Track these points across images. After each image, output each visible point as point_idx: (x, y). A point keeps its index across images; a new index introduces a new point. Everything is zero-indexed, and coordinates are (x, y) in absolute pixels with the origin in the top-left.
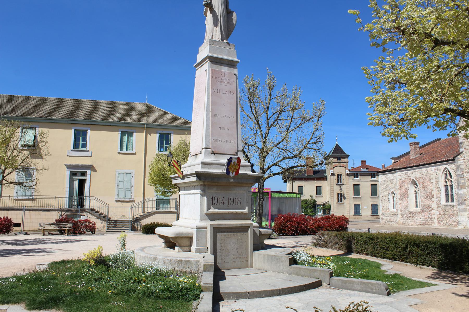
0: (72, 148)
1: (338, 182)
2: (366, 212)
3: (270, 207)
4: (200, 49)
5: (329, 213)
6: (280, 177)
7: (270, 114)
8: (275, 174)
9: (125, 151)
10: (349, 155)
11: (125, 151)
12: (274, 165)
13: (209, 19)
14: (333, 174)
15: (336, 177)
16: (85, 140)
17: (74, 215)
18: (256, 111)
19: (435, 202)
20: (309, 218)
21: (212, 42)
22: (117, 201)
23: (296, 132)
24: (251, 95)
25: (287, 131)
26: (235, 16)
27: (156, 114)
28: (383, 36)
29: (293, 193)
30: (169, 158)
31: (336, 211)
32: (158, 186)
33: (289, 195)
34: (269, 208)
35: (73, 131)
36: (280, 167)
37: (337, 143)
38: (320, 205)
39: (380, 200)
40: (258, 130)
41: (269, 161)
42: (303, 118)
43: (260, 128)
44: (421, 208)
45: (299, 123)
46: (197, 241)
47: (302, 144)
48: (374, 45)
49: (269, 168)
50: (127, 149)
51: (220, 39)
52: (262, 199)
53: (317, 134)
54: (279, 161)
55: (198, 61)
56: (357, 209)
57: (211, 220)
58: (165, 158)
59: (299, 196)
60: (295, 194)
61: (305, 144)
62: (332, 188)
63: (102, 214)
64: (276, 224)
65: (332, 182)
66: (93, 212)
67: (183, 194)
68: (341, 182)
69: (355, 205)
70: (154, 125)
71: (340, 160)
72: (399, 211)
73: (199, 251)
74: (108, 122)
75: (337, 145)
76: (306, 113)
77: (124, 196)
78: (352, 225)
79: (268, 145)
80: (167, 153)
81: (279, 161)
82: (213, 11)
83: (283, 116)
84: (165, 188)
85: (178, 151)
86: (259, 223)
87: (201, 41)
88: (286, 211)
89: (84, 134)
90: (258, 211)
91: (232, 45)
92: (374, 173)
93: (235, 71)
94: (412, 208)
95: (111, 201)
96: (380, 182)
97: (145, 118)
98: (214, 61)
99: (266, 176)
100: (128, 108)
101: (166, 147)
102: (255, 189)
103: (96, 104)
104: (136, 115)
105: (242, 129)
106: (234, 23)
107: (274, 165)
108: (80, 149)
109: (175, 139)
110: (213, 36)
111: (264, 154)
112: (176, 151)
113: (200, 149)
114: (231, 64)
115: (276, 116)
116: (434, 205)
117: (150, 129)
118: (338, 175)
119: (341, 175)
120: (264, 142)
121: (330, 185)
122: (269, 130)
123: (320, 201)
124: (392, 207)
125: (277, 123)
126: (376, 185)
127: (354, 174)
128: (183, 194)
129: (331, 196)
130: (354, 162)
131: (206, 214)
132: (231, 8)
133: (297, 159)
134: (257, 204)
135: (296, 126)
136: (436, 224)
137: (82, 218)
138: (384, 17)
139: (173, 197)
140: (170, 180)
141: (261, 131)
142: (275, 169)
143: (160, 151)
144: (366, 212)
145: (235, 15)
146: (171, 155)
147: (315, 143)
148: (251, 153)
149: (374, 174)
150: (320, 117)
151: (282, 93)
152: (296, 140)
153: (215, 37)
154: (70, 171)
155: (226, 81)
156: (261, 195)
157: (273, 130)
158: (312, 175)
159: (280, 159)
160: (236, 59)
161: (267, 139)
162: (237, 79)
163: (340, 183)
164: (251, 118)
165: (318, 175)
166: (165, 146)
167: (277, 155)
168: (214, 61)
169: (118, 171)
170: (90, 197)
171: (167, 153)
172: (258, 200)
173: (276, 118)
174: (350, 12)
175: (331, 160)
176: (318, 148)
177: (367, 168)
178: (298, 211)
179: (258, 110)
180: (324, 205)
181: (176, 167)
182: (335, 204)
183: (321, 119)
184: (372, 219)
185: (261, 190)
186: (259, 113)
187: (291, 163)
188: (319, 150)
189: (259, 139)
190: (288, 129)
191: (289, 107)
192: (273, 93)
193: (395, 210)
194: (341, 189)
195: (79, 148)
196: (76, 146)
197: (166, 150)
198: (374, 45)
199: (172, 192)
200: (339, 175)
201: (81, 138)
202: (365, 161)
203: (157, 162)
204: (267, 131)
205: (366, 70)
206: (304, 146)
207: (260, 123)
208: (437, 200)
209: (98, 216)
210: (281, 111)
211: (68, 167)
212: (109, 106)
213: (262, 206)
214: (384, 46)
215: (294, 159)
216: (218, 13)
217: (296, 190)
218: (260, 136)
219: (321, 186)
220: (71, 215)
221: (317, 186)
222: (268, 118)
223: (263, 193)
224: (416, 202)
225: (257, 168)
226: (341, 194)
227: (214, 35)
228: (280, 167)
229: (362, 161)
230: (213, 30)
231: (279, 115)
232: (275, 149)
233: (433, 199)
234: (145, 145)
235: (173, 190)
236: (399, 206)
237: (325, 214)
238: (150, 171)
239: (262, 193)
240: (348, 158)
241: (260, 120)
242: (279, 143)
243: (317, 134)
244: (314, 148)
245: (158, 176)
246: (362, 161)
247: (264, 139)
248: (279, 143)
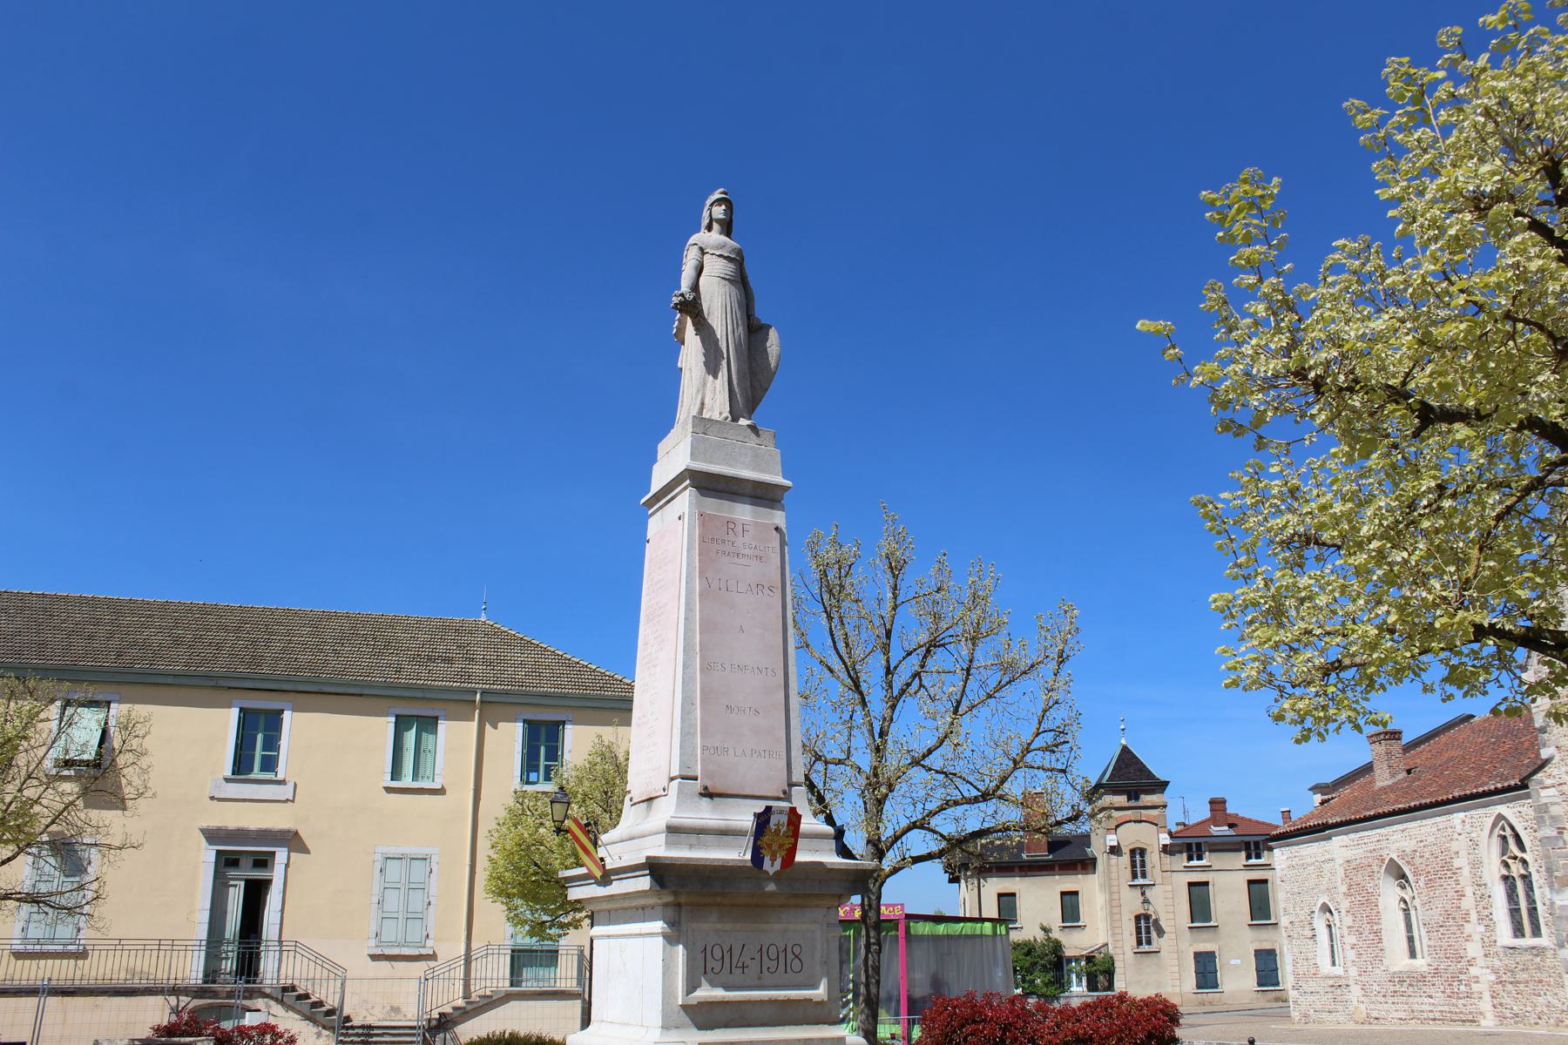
0: (229, 773)
1: (1134, 876)
2: (1238, 978)
3: (903, 973)
4: (662, 447)
5: (1110, 987)
6: (936, 867)
7: (896, 654)
8: (917, 860)
9: (407, 781)
10: (1166, 783)
11: (407, 781)
12: (913, 826)
13: (692, 352)
14: (1115, 850)
15: (1126, 859)
16: (272, 743)
17: (221, 1006)
18: (847, 645)
19: (1477, 937)
20: (1039, 1008)
21: (702, 423)
22: (374, 957)
23: (984, 711)
24: (833, 592)
25: (955, 712)
26: (773, 341)
27: (516, 655)
28: (1255, 400)
29: (982, 920)
30: (556, 806)
31: (1133, 981)
32: (520, 902)
33: (967, 928)
34: (903, 973)
35: (234, 713)
36: (935, 832)
37: (1123, 742)
38: (1077, 959)
39: (1284, 935)
40: (859, 708)
41: (896, 814)
42: (1007, 667)
43: (864, 703)
44: (1429, 960)
45: (992, 684)
47: (1006, 754)
48: (1226, 428)
49: (897, 838)
50: (415, 776)
51: (726, 413)
52: (875, 948)
53: (1057, 717)
54: (932, 814)
55: (656, 486)
56: (1206, 970)
57: (703, 1026)
58: (543, 806)
59: (1002, 930)
60: (988, 925)
61: (1015, 752)
62: (1115, 896)
63: (320, 1004)
64: (927, 1031)
65: (1114, 875)
66: (289, 995)
67: (602, 937)
68: (1144, 875)
69: (1197, 955)
70: (507, 693)
71: (1137, 798)
74: (354, 684)
75: (1125, 750)
76: (1016, 647)
77: (400, 938)
78: (1192, 1026)
79: (893, 760)
80: (550, 787)
81: (932, 814)
82: (702, 327)
83: (938, 660)
84: (543, 909)
85: (587, 784)
86: (865, 1037)
87: (665, 423)
88: (959, 986)
89: (273, 722)
90: (862, 989)
91: (766, 435)
92: (1255, 842)
93: (779, 518)
94: (1398, 960)
95: (355, 959)
96: (1278, 873)
97: (477, 669)
98: (709, 485)
99: (887, 864)
100: (422, 637)
101: (548, 769)
102: (853, 910)
103: (317, 622)
104: (449, 660)
105: (804, 706)
106: (773, 361)
107: (913, 826)
108: (256, 774)
109: (579, 742)
110: (703, 404)
111: (878, 791)
112: (580, 781)
113: (662, 777)
114: (764, 495)
115: (914, 661)
116: (1474, 949)
117: (493, 706)
118: (1133, 852)
119: (1142, 852)
120: (878, 749)
121: (1108, 887)
122: (893, 707)
123: (1075, 944)
125: (921, 686)
126: (1265, 881)
127: (1189, 847)
128: (602, 937)
129: (1114, 927)
130: (1185, 806)
131: (684, 1007)
132: (761, 314)
133: (991, 806)
134: (860, 961)
135: (982, 694)
136: (1489, 1015)
137: (250, 1020)
138: (1254, 342)
139: (569, 942)
140: (563, 884)
141: (868, 714)
142: (918, 842)
143: (528, 783)
144: (1238, 978)
145: (773, 337)
146: (563, 797)
147: (1049, 749)
148: (834, 785)
149: (1257, 844)
150: (1062, 659)
151: (934, 583)
152: (985, 739)
153: (712, 409)
154: (218, 852)
156: (872, 933)
157: (907, 706)
158: (1044, 855)
159: (932, 806)
160: (779, 479)
161: (890, 738)
162: (783, 544)
163: (1140, 881)
164: (831, 671)
165: (1064, 854)
166: (542, 763)
167: (922, 793)
168: (709, 485)
170: (280, 941)
171: (550, 787)
172: (863, 951)
173: (917, 668)
174: (1145, 329)
175: (1108, 799)
176: (1060, 767)
177: (1231, 826)
178: (1001, 984)
179: (859, 644)
180: (1090, 959)
181: (575, 837)
182: (1129, 955)
183: (1067, 668)
184: (1261, 1002)
185: (872, 914)
186: (858, 652)
187: (973, 819)
188: (1064, 771)
189: (861, 741)
190: (959, 702)
191: (959, 630)
192: (902, 585)
194: (1146, 901)
195: (251, 770)
196: (242, 765)
197: (548, 778)
198: (1226, 428)
199: (568, 925)
200: (1138, 853)
201: (260, 737)
202: (1224, 802)
203: (516, 819)
204: (887, 713)
205: (1204, 505)
206: (1015, 761)
207: (864, 687)
208: (1482, 929)
209: (306, 1009)
210: (932, 645)
211: (212, 836)
212: (358, 630)
213: (877, 970)
214: (1261, 431)
215: (983, 805)
216: (720, 333)
217: (991, 910)
218: (865, 729)
219: (1076, 893)
220: (211, 1007)
221: (1063, 894)
222: (888, 668)
223: (879, 924)
224: (1411, 939)
225: (856, 840)
226: (1147, 917)
227: (707, 401)
228: (935, 832)
229: (1212, 802)
230: (704, 384)
231: (925, 657)
232: (917, 774)
233: (1468, 928)
234: (478, 758)
235: (569, 918)
237: (1096, 990)
238: (491, 853)
239: (874, 924)
240: (1162, 791)
241: (863, 677)
242: (930, 752)
243: (1057, 717)
244: (1047, 765)
245: (517, 869)
246: (1212, 802)
247: (878, 741)
248: (930, 752)
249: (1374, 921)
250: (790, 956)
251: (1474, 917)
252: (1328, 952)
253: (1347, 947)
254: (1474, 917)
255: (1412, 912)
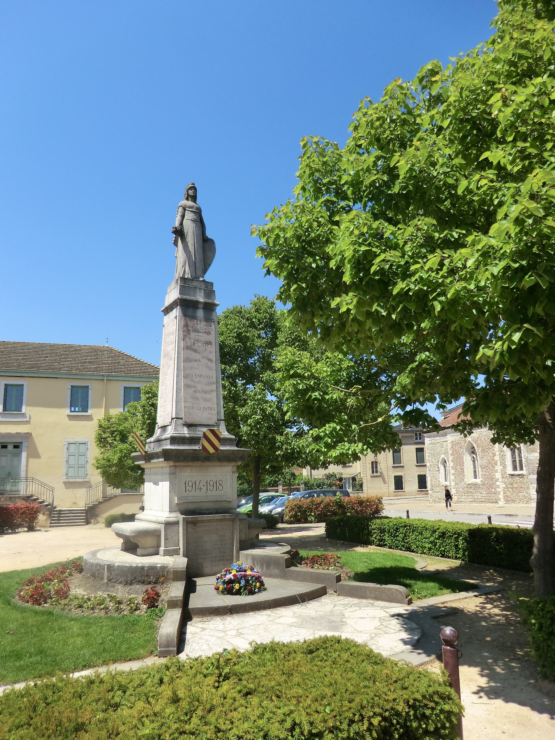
19: (499, 471)
44: (481, 479)
46: (166, 539)
72: (453, 484)
73: (167, 553)
94: (469, 479)
116: (498, 475)
124: (444, 479)
155: (202, 331)
169: (68, 440)
193: (447, 483)
208: (502, 468)
224: (475, 472)
233: (496, 467)
236: (452, 477)
249: (462, 464)
250: (218, 485)
251: (499, 463)
252: (444, 476)
253: (451, 474)
254: (499, 463)
255: (476, 461)
